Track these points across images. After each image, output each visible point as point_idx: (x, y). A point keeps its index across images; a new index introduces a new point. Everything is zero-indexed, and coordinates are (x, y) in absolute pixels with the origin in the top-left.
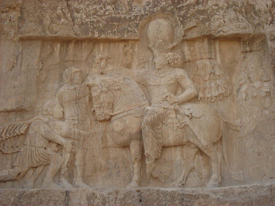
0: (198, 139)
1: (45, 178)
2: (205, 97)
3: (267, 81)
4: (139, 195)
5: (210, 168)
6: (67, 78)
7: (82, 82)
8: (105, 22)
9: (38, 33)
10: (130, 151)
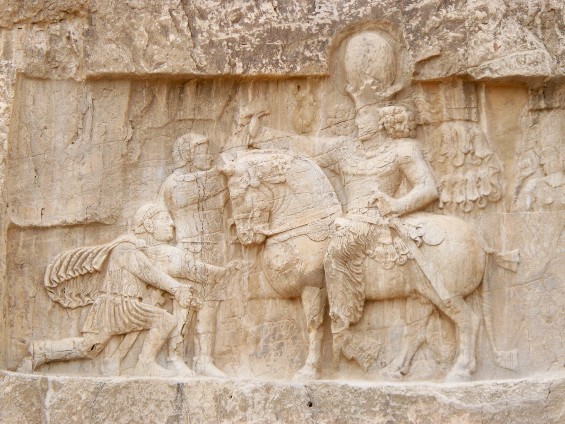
0: (432, 287)
1: (140, 355)
2: (454, 202)
4: (308, 395)
5: (456, 342)
6: (181, 158)
7: (211, 165)
8: (258, 39)
9: (124, 67)
10: (302, 307)
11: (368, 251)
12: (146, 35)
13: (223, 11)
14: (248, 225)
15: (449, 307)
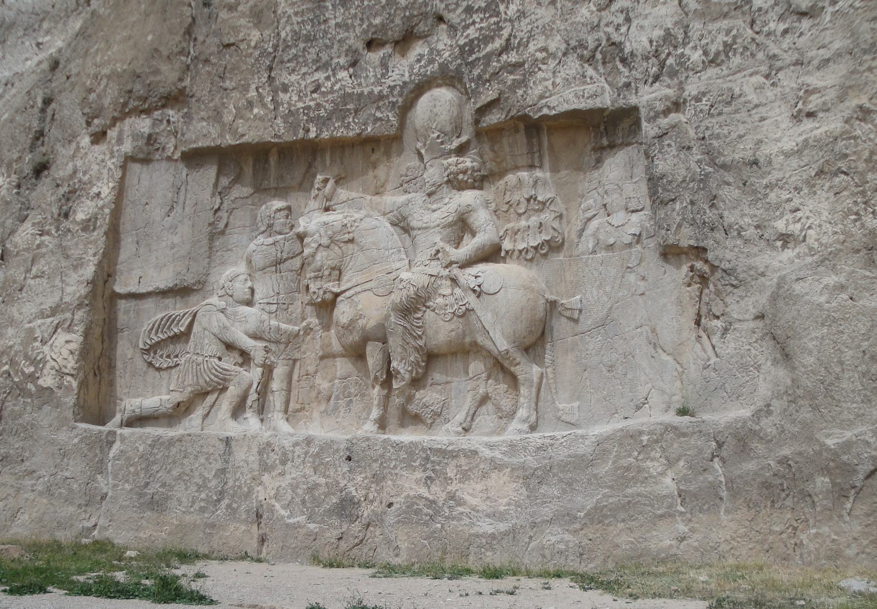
3: (637, 211)
4: (348, 449)
11: (428, 304)
12: (234, 111)
13: (303, 83)
14: (318, 283)
15: (508, 358)
